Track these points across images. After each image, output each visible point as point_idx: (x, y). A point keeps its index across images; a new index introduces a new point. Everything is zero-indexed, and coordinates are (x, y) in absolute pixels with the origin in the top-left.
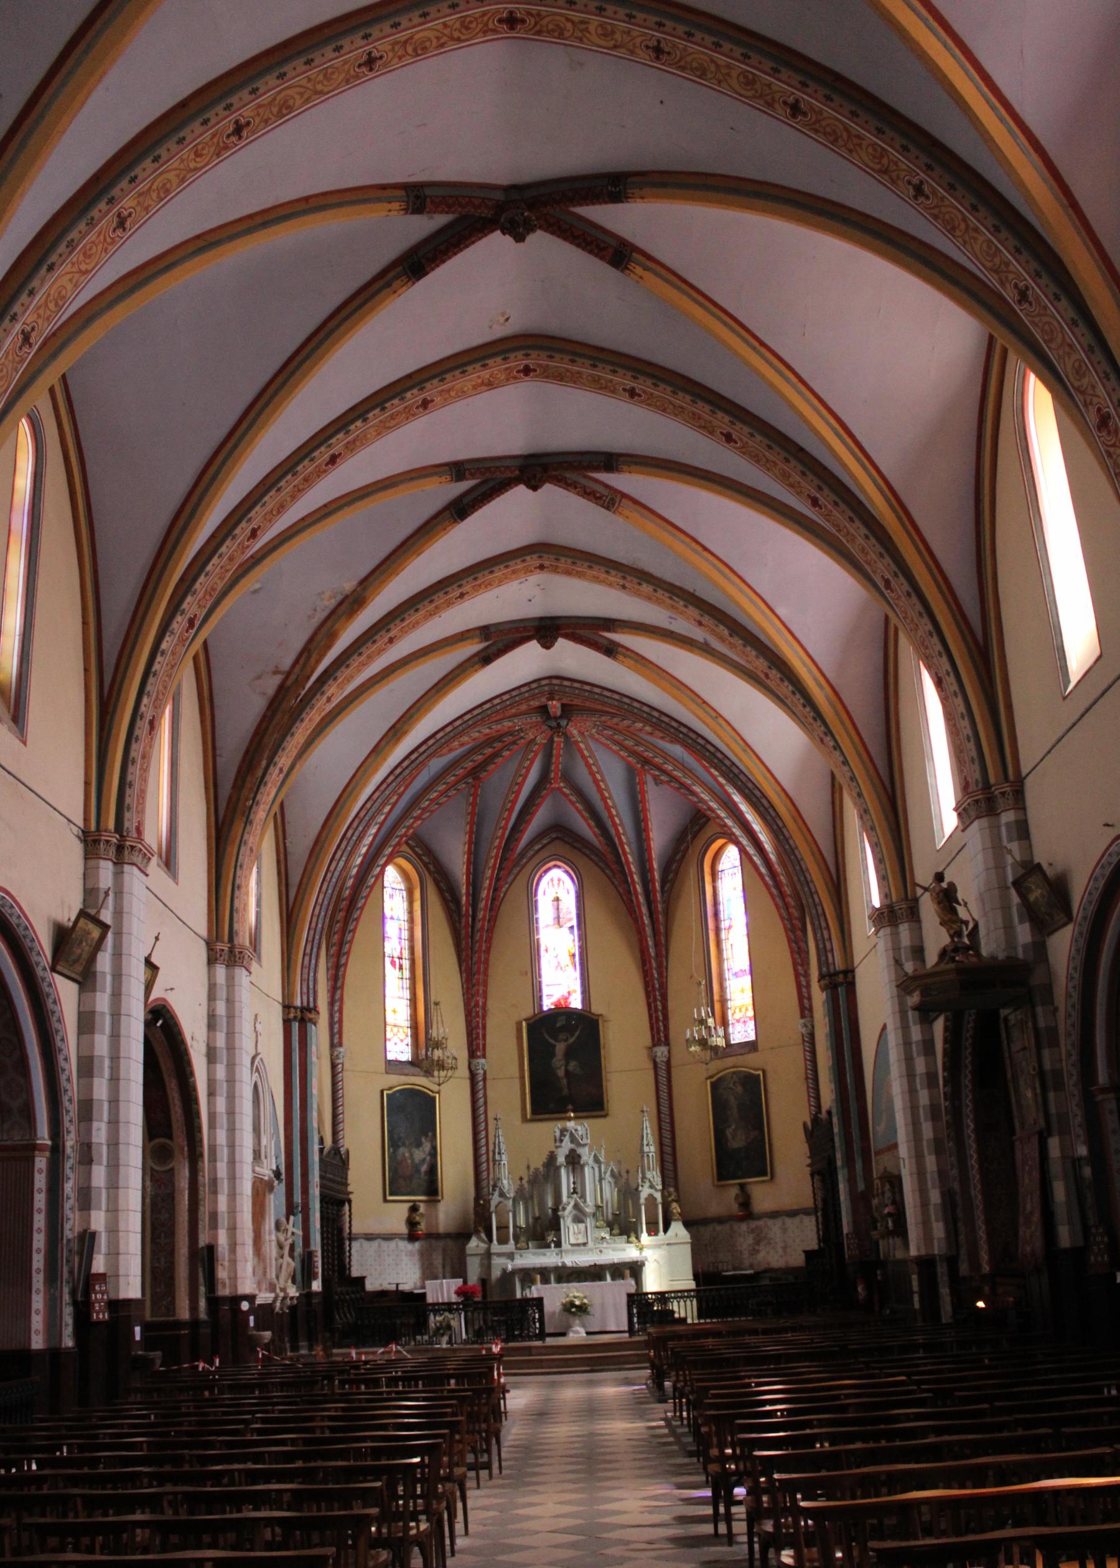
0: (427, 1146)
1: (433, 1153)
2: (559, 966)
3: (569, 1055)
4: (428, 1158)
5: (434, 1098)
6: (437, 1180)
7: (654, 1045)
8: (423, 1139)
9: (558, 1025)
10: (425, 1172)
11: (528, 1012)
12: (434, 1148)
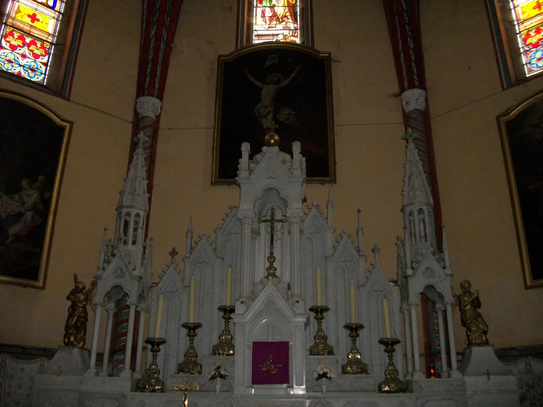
0: (31, 197)
1: (43, 209)
2: (274, 16)
3: (280, 100)
4: (29, 215)
5: (63, 129)
6: (40, 254)
7: (402, 90)
8: (24, 183)
9: (267, 64)
10: (17, 237)
11: (228, 48)
12: (47, 203)
